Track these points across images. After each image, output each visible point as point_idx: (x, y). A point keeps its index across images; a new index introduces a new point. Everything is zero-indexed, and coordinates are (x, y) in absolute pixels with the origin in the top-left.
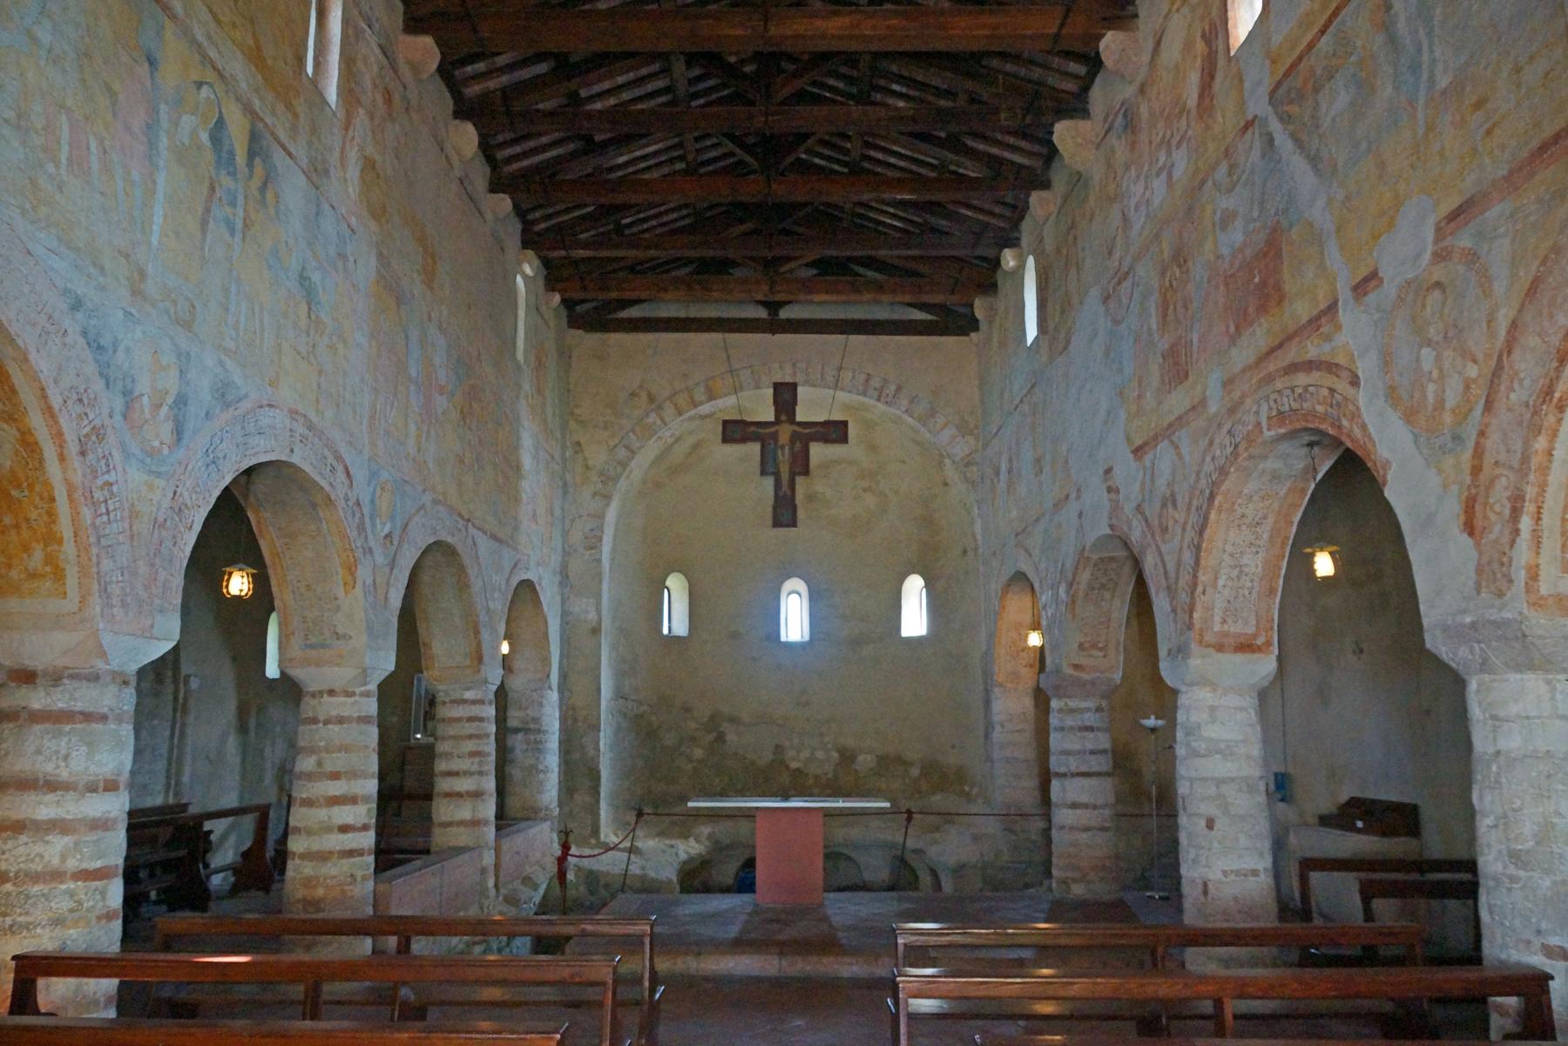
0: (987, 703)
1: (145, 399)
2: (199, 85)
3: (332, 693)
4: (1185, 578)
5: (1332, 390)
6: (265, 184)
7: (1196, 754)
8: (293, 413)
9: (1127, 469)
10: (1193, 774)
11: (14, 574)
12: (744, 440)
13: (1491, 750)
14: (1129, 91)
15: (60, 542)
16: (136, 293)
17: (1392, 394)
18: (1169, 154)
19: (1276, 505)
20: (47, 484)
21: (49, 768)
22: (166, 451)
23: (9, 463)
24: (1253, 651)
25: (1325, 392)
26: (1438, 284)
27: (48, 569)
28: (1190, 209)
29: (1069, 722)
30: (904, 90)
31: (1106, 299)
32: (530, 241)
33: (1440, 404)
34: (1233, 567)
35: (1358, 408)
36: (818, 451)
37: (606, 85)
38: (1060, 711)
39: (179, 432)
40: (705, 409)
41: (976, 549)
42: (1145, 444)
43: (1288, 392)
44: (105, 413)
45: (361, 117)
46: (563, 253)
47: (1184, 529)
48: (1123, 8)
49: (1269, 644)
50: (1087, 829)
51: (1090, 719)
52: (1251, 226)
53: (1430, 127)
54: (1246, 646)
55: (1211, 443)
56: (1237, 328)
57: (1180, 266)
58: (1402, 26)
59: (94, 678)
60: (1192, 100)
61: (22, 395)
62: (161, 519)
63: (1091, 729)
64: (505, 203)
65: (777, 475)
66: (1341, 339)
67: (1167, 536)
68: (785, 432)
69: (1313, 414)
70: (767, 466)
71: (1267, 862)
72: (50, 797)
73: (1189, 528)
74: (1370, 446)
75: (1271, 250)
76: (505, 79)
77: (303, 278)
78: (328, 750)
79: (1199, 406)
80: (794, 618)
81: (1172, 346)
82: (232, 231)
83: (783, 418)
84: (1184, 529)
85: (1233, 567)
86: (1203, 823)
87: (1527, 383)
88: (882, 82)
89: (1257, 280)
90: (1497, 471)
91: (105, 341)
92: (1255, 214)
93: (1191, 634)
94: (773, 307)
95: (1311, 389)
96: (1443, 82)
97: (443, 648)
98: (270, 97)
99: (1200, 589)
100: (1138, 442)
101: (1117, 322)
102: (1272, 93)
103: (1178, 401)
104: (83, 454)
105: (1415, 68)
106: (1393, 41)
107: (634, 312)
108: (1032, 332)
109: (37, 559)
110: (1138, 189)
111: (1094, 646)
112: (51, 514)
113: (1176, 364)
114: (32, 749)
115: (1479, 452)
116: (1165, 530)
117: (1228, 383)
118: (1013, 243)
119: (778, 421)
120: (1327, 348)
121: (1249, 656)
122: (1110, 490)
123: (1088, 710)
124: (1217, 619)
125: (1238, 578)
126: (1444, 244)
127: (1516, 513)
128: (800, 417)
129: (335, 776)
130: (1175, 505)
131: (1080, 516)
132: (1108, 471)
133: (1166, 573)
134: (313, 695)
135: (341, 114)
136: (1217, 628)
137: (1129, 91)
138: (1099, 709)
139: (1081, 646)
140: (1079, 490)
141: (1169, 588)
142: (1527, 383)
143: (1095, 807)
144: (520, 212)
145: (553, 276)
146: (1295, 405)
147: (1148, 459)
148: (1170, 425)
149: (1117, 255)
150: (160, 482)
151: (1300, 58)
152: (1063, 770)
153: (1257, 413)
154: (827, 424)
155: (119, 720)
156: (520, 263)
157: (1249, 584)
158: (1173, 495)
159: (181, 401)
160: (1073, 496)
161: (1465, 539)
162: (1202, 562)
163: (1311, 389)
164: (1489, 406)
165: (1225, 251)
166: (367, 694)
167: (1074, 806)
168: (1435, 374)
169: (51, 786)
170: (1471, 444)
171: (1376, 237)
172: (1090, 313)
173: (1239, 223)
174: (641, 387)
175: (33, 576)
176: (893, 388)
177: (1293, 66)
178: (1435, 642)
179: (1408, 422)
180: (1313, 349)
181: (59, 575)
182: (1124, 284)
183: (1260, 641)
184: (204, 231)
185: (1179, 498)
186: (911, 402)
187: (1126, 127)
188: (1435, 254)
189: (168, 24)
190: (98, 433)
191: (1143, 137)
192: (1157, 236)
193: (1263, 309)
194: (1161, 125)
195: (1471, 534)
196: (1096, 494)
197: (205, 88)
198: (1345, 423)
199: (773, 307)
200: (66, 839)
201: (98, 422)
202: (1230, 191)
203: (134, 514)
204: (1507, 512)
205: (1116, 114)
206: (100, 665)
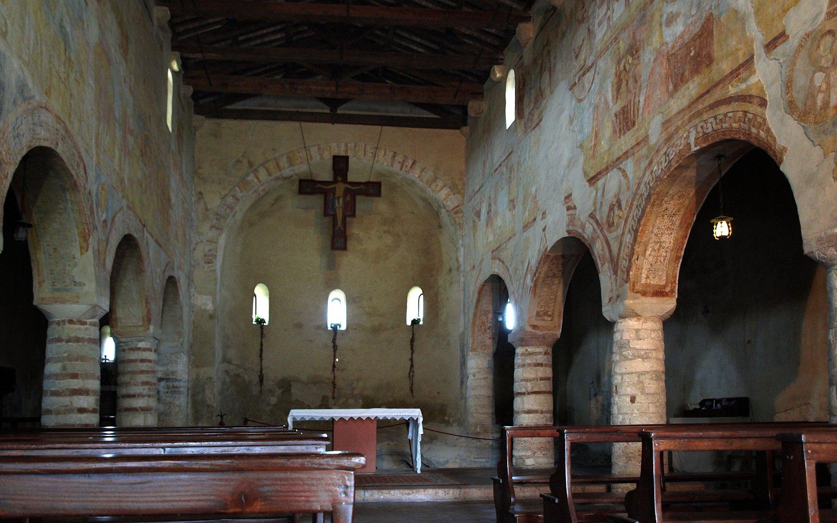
0: (463, 364)
4: (625, 252)
5: (745, 112)
7: (626, 358)
10: (624, 370)
12: (313, 193)
17: (791, 107)
19: (687, 202)
24: (663, 296)
26: (830, 32)
29: (528, 361)
34: (656, 243)
35: (765, 120)
36: (362, 203)
38: (523, 354)
40: (287, 172)
41: (458, 268)
42: (600, 173)
46: (199, 56)
47: (626, 221)
49: (672, 291)
51: (541, 359)
54: (659, 293)
55: (650, 163)
63: (541, 365)
65: (334, 217)
67: (612, 229)
68: (340, 188)
69: (730, 130)
70: (328, 210)
73: (630, 219)
74: (772, 142)
75: (705, 33)
80: (337, 311)
81: (623, 109)
83: (339, 179)
84: (626, 221)
85: (656, 243)
89: (692, 54)
92: (694, 12)
93: (628, 285)
99: (635, 257)
103: (627, 141)
107: (239, 106)
111: (546, 314)
116: (611, 225)
117: (666, 124)
119: (335, 181)
120: (743, 86)
121: (660, 299)
122: (569, 208)
123: (540, 353)
124: (644, 276)
125: (659, 250)
128: (351, 177)
131: (544, 230)
132: (568, 197)
136: (643, 281)
138: (546, 353)
140: (544, 213)
143: (542, 412)
147: (600, 183)
148: (618, 159)
152: (523, 390)
153: (688, 137)
154: (368, 184)
160: (539, 217)
162: (639, 239)
167: (529, 412)
168: (824, 87)
173: (680, 20)
174: (243, 156)
176: (410, 162)
185: (624, 204)
186: (422, 171)
192: (616, 39)
193: (696, 71)
198: (754, 130)
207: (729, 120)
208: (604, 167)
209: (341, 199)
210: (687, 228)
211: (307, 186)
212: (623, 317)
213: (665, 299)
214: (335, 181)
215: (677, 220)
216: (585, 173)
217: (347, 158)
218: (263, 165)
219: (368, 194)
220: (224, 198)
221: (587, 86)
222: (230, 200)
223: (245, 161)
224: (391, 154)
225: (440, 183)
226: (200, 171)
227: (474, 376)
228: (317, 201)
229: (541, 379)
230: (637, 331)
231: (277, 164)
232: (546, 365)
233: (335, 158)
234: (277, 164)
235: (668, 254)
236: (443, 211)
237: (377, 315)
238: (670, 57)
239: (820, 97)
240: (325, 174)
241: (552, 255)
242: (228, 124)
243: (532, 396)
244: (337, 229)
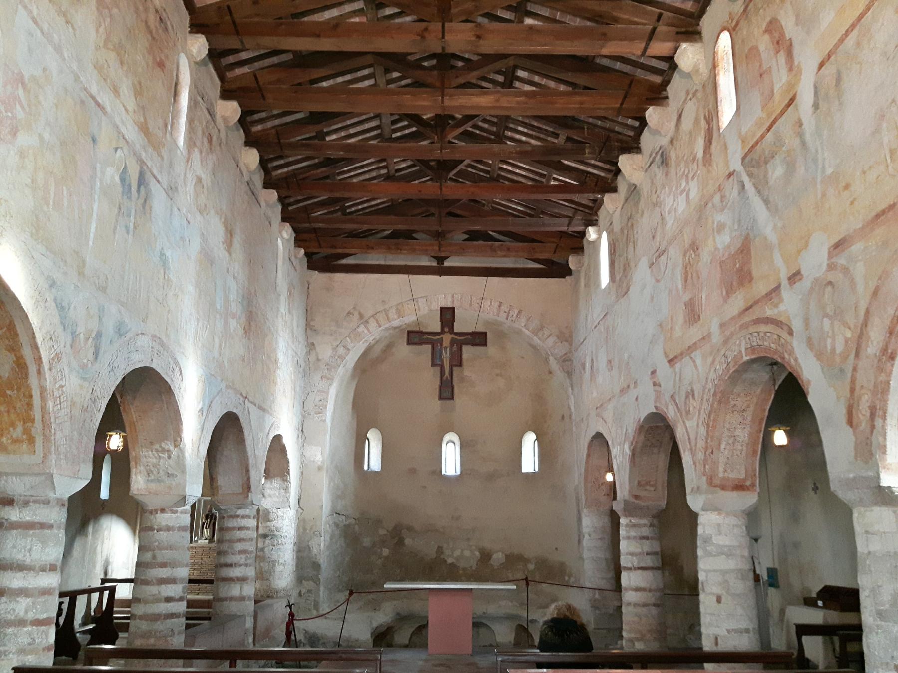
0: (579, 520)
1: (82, 335)
2: (116, 149)
3: (163, 511)
6: (145, 201)
8: (154, 337)
11: (4, 439)
13: (866, 552)
14: (664, 141)
15: (33, 421)
16: (81, 274)
17: (809, 342)
18: (687, 183)
19: (755, 399)
21: (20, 557)
22: (90, 365)
23: (7, 375)
25: (776, 337)
26: (830, 283)
27: (25, 437)
28: (700, 219)
30: (526, 130)
32: (286, 218)
33: (833, 350)
36: (468, 352)
37: (340, 125)
39: (96, 354)
40: (396, 323)
41: (570, 416)
42: (676, 357)
43: (756, 334)
44: (62, 346)
45: (196, 154)
48: (660, 93)
49: (753, 485)
52: (734, 235)
53: (824, 195)
54: (739, 487)
56: (727, 292)
57: (694, 251)
58: (808, 137)
59: (47, 502)
60: (700, 155)
61: (21, 336)
62: (85, 406)
63: (647, 538)
64: (273, 195)
65: (442, 367)
66: (782, 307)
68: (447, 338)
69: (768, 349)
70: (435, 361)
71: (752, 625)
72: (20, 575)
73: (702, 411)
75: (745, 249)
76: (277, 122)
77: (162, 254)
78: (160, 549)
79: (706, 338)
80: (451, 461)
81: (691, 299)
82: (128, 232)
83: (446, 329)
86: (715, 599)
87: (875, 343)
88: (512, 125)
90: (862, 392)
91: (65, 304)
92: (736, 227)
94: (440, 260)
95: (768, 334)
96: (829, 171)
97: (227, 482)
98: (150, 150)
100: (671, 357)
101: (658, 281)
102: (743, 159)
104: (50, 369)
105: (815, 160)
106: (804, 143)
109: (18, 432)
110: (669, 202)
111: (648, 483)
112: (30, 405)
113: (693, 310)
114: (11, 545)
115: (853, 381)
116: (688, 412)
117: (722, 325)
118: (593, 223)
119: (442, 332)
120: (776, 311)
122: (655, 384)
123: (645, 525)
124: (721, 469)
126: (833, 260)
128: (457, 328)
129: (163, 565)
130: (693, 395)
131: (637, 399)
133: (689, 439)
134: (151, 513)
135: (185, 153)
136: (721, 475)
137: (664, 141)
138: (651, 525)
139: (639, 482)
141: (691, 449)
142: (875, 343)
144: (281, 199)
146: (760, 343)
147: (678, 366)
149: (658, 238)
150: (86, 384)
151: (757, 143)
152: (630, 565)
153: (740, 345)
154: (474, 334)
155: (59, 528)
156: (280, 232)
157: (740, 448)
158: (693, 391)
159: (99, 335)
160: (632, 386)
163: (768, 334)
164: (857, 355)
165: (720, 246)
166: (184, 512)
168: (830, 334)
169: (21, 567)
170: (849, 375)
171: (799, 252)
172: (641, 273)
173: (727, 230)
176: (516, 311)
177: (753, 147)
179: (818, 359)
180: (769, 312)
181: (31, 440)
182: (662, 257)
183: (748, 483)
184: (114, 233)
186: (528, 320)
187: (662, 162)
188: (828, 265)
189: (104, 118)
190: (58, 357)
191: (672, 170)
193: (741, 283)
194: (682, 165)
195: (851, 426)
196: (645, 389)
197: (119, 151)
198: (786, 356)
200: (28, 600)
201: (58, 351)
202: (722, 210)
203: (73, 404)
204: (868, 414)
205: (656, 153)
206: (51, 495)
207: (768, 340)
208: (679, 352)
209: (448, 350)
210: (760, 423)
211: (415, 336)
213: (744, 493)
214: (442, 332)
215: (749, 415)
217: (453, 309)
218: (373, 316)
219: (474, 345)
220: (335, 349)
221: (662, 268)
222: (341, 351)
223: (356, 313)
224: (498, 303)
225: (547, 332)
226: (312, 323)
229: (647, 554)
230: (719, 525)
231: (387, 316)
232: (652, 539)
233: (442, 309)
234: (387, 316)
235: (745, 448)
236: (551, 358)
237: (490, 465)
238: (722, 263)
239: (829, 341)
241: (646, 426)
242: (340, 277)
243: (640, 572)
244: (444, 378)
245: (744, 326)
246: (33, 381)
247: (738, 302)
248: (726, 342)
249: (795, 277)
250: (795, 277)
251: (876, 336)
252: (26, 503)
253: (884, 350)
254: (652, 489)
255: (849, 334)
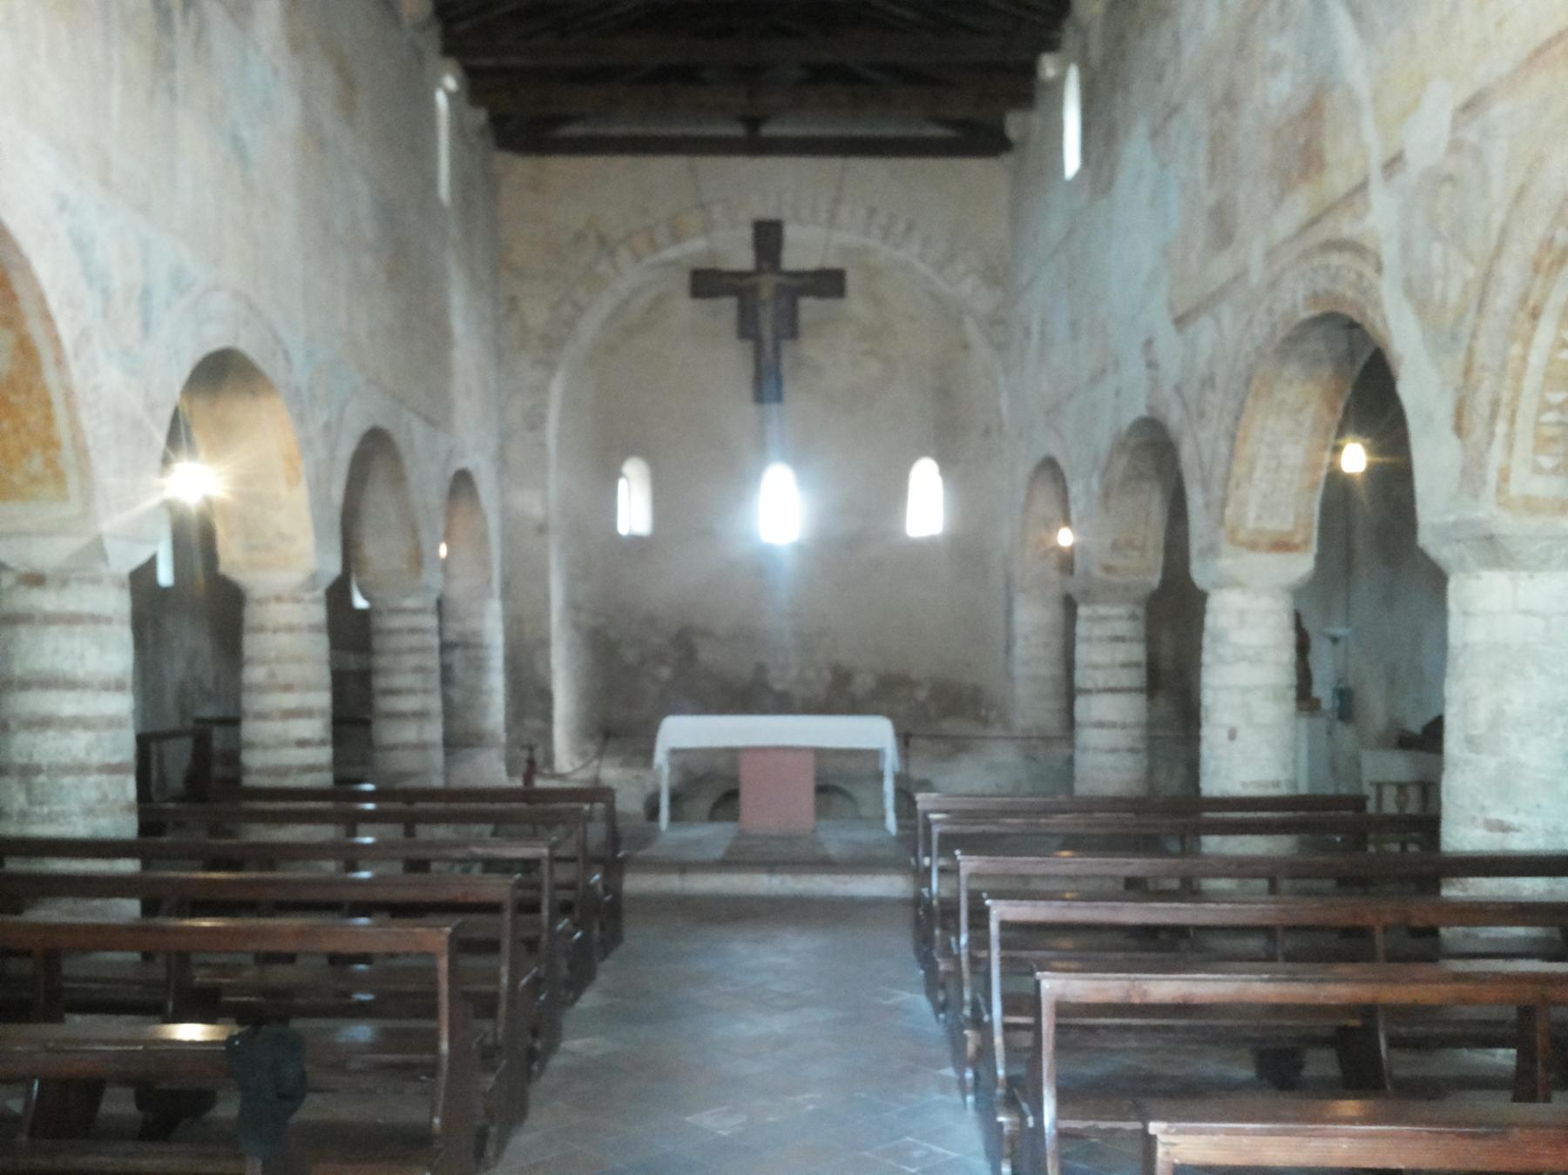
3: (279, 599)
4: (1219, 471)
9: (1169, 344)
20: (44, 390)
25: (1353, 276)
26: (1450, 178)
31: (1154, 134)
32: (452, 48)
39: (146, 326)
40: (671, 253)
49: (1306, 542)
50: (1114, 750)
51: (1122, 628)
54: (1282, 545)
70: (747, 327)
72: (70, 695)
78: (279, 660)
79: (1240, 277)
94: (753, 123)
97: (380, 551)
99: (1232, 483)
100: (1180, 312)
101: (1164, 166)
103: (1221, 268)
104: (76, 356)
108: (1072, 161)
109: (36, 464)
111: (1130, 544)
112: (49, 419)
115: (1470, 352)
116: (1202, 415)
117: (1271, 254)
118: (1052, 46)
119: (759, 271)
123: (1120, 618)
127: (1493, 416)
129: (288, 688)
131: (1117, 393)
132: (1149, 343)
136: (1251, 525)
138: (1133, 617)
143: (1124, 726)
145: (477, 86)
147: (1191, 330)
152: (1089, 685)
159: (146, 294)
161: (1454, 440)
167: (1100, 725)
169: (70, 684)
172: (1136, 150)
175: (35, 480)
176: (901, 226)
178: (1426, 539)
180: (1346, 228)
183: (1298, 539)
196: (1133, 371)
199: (753, 123)
202: (1282, 29)
212: (1220, 585)
215: (1307, 418)
216: (1171, 307)
222: (567, 309)
227: (1026, 638)
228: (728, 306)
232: (1132, 640)
240: (742, 257)
245: (1306, 255)
246: (50, 376)
247: (1299, 207)
248: (1273, 285)
249: (1393, 164)
250: (1393, 164)
251: (1511, 272)
252: (64, 583)
253: (1523, 300)
254: (1136, 553)
255: (1470, 272)
